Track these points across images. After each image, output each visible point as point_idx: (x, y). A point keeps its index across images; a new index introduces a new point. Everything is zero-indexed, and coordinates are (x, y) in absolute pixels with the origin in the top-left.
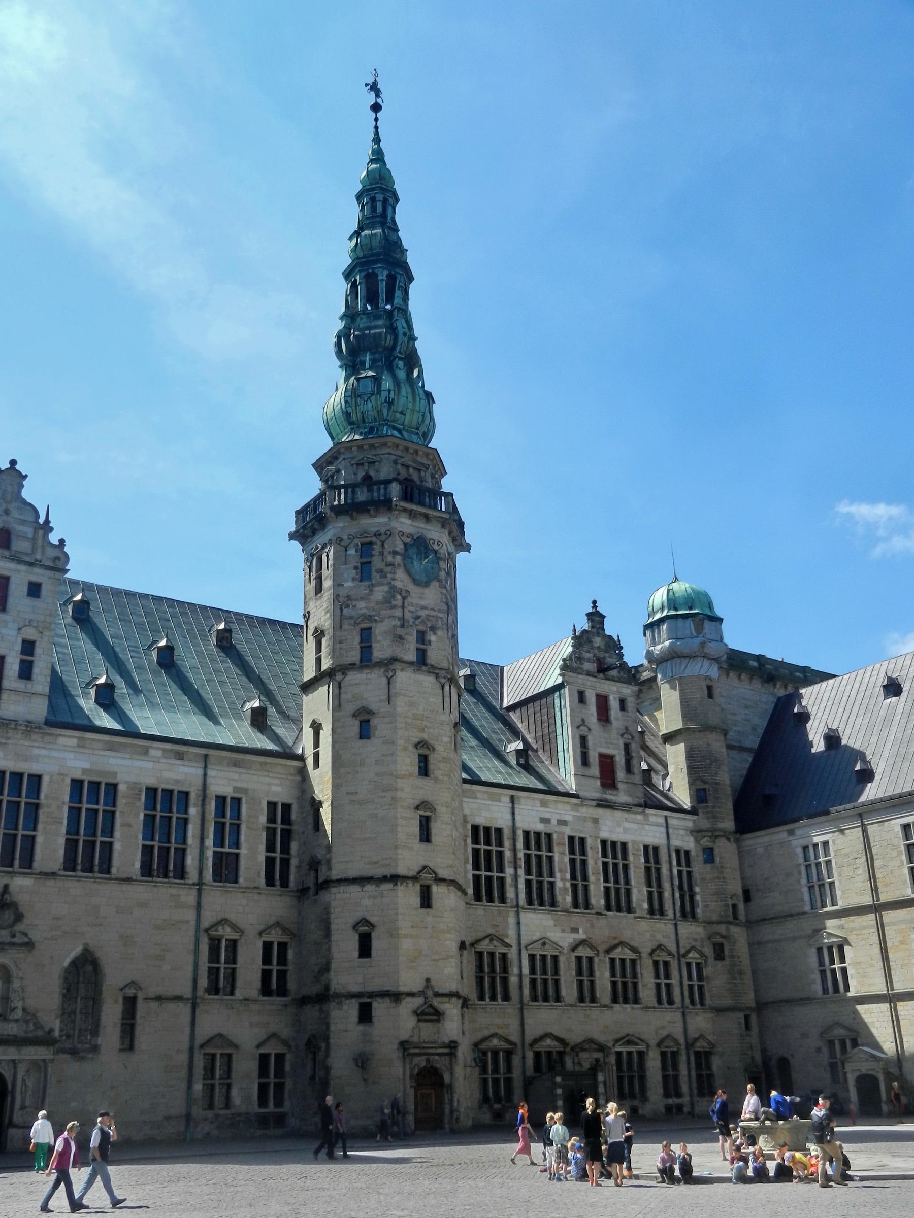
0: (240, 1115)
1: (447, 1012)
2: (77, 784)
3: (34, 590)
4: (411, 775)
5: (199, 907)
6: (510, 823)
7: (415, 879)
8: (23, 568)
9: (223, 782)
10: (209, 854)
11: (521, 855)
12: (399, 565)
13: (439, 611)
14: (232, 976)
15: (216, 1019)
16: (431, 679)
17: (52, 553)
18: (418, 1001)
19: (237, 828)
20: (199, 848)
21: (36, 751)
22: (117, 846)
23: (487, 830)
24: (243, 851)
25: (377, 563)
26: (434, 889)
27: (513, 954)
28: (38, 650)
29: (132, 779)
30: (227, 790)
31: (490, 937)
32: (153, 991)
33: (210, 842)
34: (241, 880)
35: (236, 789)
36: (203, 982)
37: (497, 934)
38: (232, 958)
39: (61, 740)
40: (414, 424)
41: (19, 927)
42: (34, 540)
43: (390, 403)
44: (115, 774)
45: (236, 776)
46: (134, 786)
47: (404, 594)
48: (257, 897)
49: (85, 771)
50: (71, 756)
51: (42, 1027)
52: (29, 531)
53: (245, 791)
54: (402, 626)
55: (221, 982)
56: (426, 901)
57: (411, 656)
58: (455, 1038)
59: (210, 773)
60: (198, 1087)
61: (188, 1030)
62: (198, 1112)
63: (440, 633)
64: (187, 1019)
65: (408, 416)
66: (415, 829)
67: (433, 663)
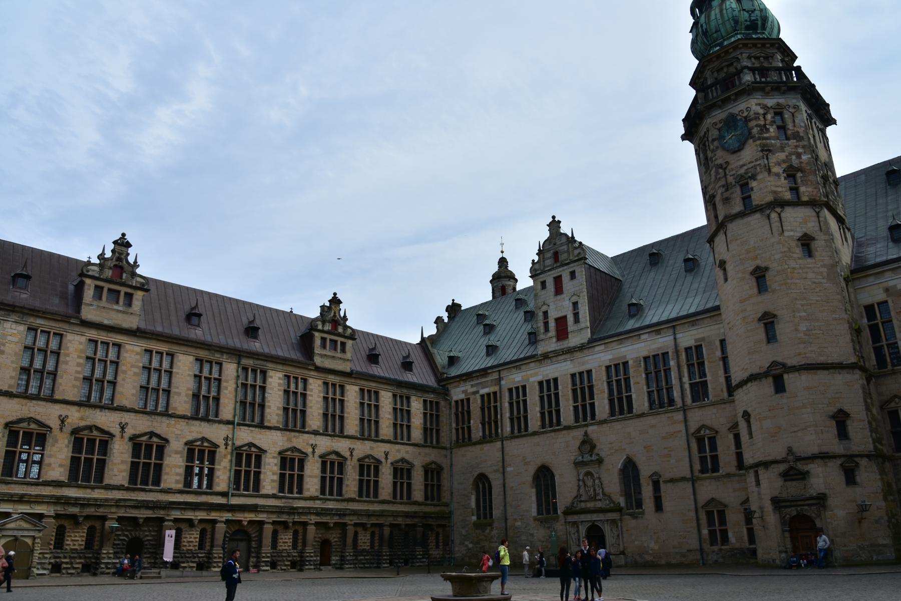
0: (736, 549)
2: (608, 368)
3: (573, 275)
5: (686, 420)
9: (687, 338)
10: (687, 386)
12: (717, 148)
13: (756, 160)
14: (715, 459)
15: (708, 490)
16: (757, 216)
17: (576, 252)
18: (782, 467)
19: (701, 364)
20: (680, 383)
21: (587, 358)
22: (634, 396)
24: (709, 378)
25: (709, 154)
26: (786, 376)
28: (580, 306)
29: (635, 356)
30: (691, 343)
32: (667, 475)
33: (686, 379)
35: (696, 340)
36: (697, 466)
38: (714, 447)
39: (597, 349)
40: (730, 30)
41: (596, 451)
42: (568, 252)
43: (705, 33)
45: (695, 332)
46: (637, 360)
47: (724, 166)
48: (723, 406)
50: (602, 354)
51: (614, 502)
52: (565, 248)
53: (703, 339)
54: (727, 190)
55: (709, 464)
56: (780, 387)
57: (738, 207)
59: (678, 336)
60: (705, 532)
61: (692, 497)
62: (706, 546)
63: (759, 177)
64: (690, 490)
65: (722, 30)
66: (761, 335)
67: (757, 203)
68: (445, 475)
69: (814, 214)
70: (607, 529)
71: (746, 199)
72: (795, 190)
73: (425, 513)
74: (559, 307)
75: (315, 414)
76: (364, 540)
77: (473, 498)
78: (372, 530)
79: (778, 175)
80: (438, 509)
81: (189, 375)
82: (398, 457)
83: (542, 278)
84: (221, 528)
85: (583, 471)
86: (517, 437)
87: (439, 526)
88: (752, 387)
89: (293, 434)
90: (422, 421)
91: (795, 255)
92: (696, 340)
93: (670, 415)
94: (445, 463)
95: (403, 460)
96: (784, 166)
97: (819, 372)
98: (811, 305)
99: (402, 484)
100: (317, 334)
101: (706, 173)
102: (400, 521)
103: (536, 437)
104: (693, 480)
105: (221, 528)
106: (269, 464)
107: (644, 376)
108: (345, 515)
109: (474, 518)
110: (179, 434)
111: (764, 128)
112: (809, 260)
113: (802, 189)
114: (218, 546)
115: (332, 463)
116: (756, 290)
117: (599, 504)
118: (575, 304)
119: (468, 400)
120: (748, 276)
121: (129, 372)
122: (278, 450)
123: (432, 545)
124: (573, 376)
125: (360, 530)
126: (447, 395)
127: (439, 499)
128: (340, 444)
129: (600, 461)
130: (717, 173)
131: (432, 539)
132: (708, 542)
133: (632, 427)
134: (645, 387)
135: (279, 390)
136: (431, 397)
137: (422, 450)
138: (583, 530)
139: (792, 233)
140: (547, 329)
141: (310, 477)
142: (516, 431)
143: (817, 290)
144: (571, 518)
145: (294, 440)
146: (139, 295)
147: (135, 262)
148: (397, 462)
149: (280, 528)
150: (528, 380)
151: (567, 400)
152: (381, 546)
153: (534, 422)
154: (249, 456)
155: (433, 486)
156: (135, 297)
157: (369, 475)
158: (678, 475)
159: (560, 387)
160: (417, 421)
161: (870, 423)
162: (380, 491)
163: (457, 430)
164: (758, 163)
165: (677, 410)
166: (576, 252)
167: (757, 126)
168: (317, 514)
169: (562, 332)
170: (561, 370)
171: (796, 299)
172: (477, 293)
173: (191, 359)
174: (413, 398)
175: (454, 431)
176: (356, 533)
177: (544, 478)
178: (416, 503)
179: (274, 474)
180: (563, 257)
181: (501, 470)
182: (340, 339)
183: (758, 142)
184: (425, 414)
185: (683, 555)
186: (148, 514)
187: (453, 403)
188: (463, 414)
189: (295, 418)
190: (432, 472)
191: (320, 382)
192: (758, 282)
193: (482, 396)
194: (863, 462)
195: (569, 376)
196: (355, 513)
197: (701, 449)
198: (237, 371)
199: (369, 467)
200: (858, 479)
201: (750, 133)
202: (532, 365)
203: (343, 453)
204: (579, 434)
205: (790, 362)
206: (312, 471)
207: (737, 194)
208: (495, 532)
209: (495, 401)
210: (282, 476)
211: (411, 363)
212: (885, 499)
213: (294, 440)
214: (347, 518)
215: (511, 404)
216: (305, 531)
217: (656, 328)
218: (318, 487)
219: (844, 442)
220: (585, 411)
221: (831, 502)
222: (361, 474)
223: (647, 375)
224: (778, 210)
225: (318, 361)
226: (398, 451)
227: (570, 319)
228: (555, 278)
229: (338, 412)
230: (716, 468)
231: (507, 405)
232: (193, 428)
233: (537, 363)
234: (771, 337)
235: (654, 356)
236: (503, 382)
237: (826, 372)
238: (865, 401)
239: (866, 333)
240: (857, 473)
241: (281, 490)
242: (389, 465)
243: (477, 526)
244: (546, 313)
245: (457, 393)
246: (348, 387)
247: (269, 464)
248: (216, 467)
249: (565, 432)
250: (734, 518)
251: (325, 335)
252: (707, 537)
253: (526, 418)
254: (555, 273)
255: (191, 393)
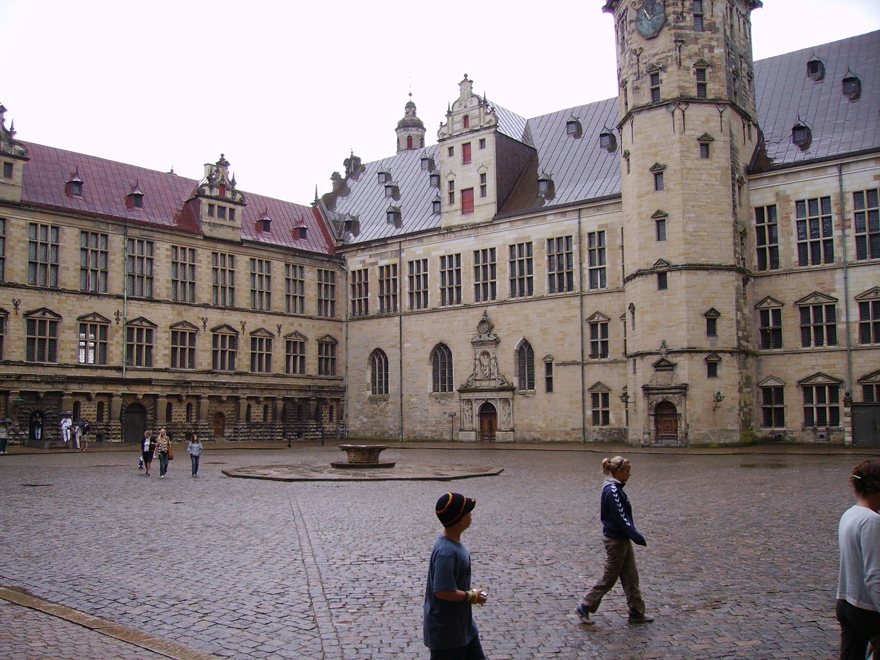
1: (680, 364)
2: (512, 247)
4: (648, 193)
6: (838, 190)
7: (651, 272)
8: (475, 134)
9: (592, 222)
10: (586, 273)
11: (851, 216)
13: (669, 51)
14: (605, 344)
15: (597, 374)
16: (663, 110)
17: (488, 118)
18: (656, 358)
19: (601, 251)
20: (580, 267)
23: (812, 201)
24: (607, 266)
26: (668, 274)
27: (840, 306)
29: (539, 237)
30: (595, 229)
31: (815, 294)
32: (559, 358)
33: (586, 265)
34: (607, 285)
35: (600, 226)
36: (588, 351)
37: (822, 291)
39: (502, 226)
41: (494, 331)
44: (529, 237)
46: (540, 241)
48: (617, 294)
49: (515, 239)
52: (476, 112)
53: (606, 225)
56: (662, 284)
57: (647, 99)
58: (686, 382)
59: (582, 220)
60: (589, 413)
62: (589, 427)
63: (669, 70)
66: (653, 233)
68: (340, 348)
69: (718, 113)
70: (499, 407)
71: (655, 91)
72: (702, 87)
73: (320, 387)
74: (466, 177)
75: (205, 286)
76: (257, 412)
77: (369, 373)
78: (265, 403)
79: (687, 69)
80: (332, 383)
81: (76, 249)
82: (292, 330)
83: (449, 143)
84: (117, 402)
85: (480, 350)
86: (417, 313)
87: (333, 400)
88: (638, 281)
89: (183, 307)
90: (316, 292)
91: (693, 156)
92: (600, 226)
93: (567, 299)
94: (340, 337)
95: (296, 333)
96: (695, 59)
97: (698, 272)
98: (700, 206)
99: (295, 357)
100: (204, 201)
101: (622, 54)
102: (293, 394)
103: (436, 314)
104: (583, 364)
105: (117, 402)
106: (160, 339)
107: (546, 258)
108: (238, 389)
109: (370, 393)
110: (71, 309)
111: (680, 16)
112: (706, 161)
113: (710, 86)
114: (115, 419)
115: (224, 337)
116: (653, 187)
117: (493, 384)
118: (483, 176)
119: (366, 271)
120: (647, 172)
121: (16, 248)
122: (169, 324)
123: (326, 419)
124: (476, 253)
125: (253, 403)
126: (343, 264)
127: (334, 373)
128: (230, 318)
129: (497, 342)
130: (631, 59)
131: (325, 413)
132: (591, 422)
133: (532, 308)
134: (546, 270)
135: (167, 262)
136: (327, 267)
137: (316, 323)
138: (476, 407)
139: (693, 132)
140: (452, 201)
141: (202, 351)
142: (415, 306)
143: (709, 192)
144: (466, 396)
145: (184, 314)
146: (19, 165)
147: (12, 128)
148: (290, 335)
149: (174, 402)
150: (430, 254)
151: (469, 278)
152: (274, 418)
153: (434, 298)
154: (140, 331)
155: (327, 359)
156: (14, 167)
157: (261, 349)
158: (570, 359)
159: (462, 264)
160: (311, 292)
161: (738, 322)
162: (273, 365)
163: (353, 302)
164: (670, 54)
165: (575, 296)
166: (488, 118)
167: (674, 13)
168: (210, 388)
169: (467, 206)
170: (465, 246)
171: (688, 200)
172: (379, 146)
173: (76, 231)
174: (306, 269)
175: (350, 303)
176: (249, 406)
177: (441, 355)
178: (310, 377)
179: (165, 348)
180: (473, 123)
181: (399, 346)
182: (228, 206)
183: (673, 31)
184: (320, 285)
185: (567, 433)
186: (48, 388)
187: (350, 274)
188: (360, 285)
189: (184, 290)
190: (327, 346)
191: (209, 253)
192: (656, 179)
193: (381, 268)
194: (726, 357)
195: (472, 253)
196: (248, 386)
197: (594, 334)
198: (124, 243)
199: (261, 340)
200: (719, 372)
201: (666, 20)
202: (435, 238)
203: (234, 327)
204: (478, 314)
205: (674, 261)
206: (204, 345)
207: (646, 84)
208: (390, 407)
209: (395, 274)
210: (174, 350)
211: (304, 230)
212: (740, 391)
213: (184, 314)
214: (240, 391)
215: (411, 278)
216: (199, 404)
217: (563, 209)
218: (210, 361)
219: (711, 338)
220: (486, 289)
221: (691, 392)
222: (253, 347)
223: (549, 257)
224: (683, 107)
225: (206, 230)
226: (292, 324)
227: (477, 192)
228: (463, 145)
229: (228, 284)
230: (605, 354)
231: (406, 279)
232: (84, 304)
233: (441, 237)
234: (660, 236)
235: (558, 239)
236: (403, 255)
237: (705, 273)
238: (737, 301)
239: (753, 235)
240: (718, 367)
241: (173, 364)
242: (282, 339)
243: (372, 400)
244: (451, 183)
245: (354, 263)
246: (238, 257)
247: (160, 339)
248: (109, 342)
249: (465, 310)
250: (614, 400)
251: (213, 202)
252: (591, 417)
253: (426, 293)
254: (464, 139)
255: (79, 267)
